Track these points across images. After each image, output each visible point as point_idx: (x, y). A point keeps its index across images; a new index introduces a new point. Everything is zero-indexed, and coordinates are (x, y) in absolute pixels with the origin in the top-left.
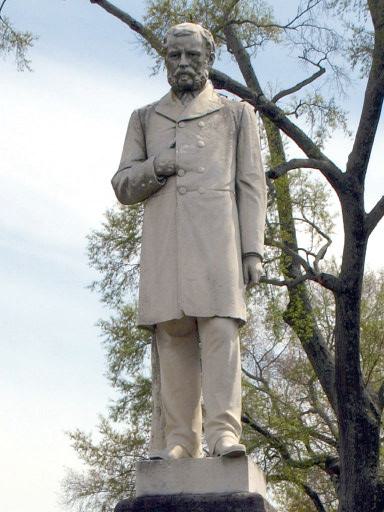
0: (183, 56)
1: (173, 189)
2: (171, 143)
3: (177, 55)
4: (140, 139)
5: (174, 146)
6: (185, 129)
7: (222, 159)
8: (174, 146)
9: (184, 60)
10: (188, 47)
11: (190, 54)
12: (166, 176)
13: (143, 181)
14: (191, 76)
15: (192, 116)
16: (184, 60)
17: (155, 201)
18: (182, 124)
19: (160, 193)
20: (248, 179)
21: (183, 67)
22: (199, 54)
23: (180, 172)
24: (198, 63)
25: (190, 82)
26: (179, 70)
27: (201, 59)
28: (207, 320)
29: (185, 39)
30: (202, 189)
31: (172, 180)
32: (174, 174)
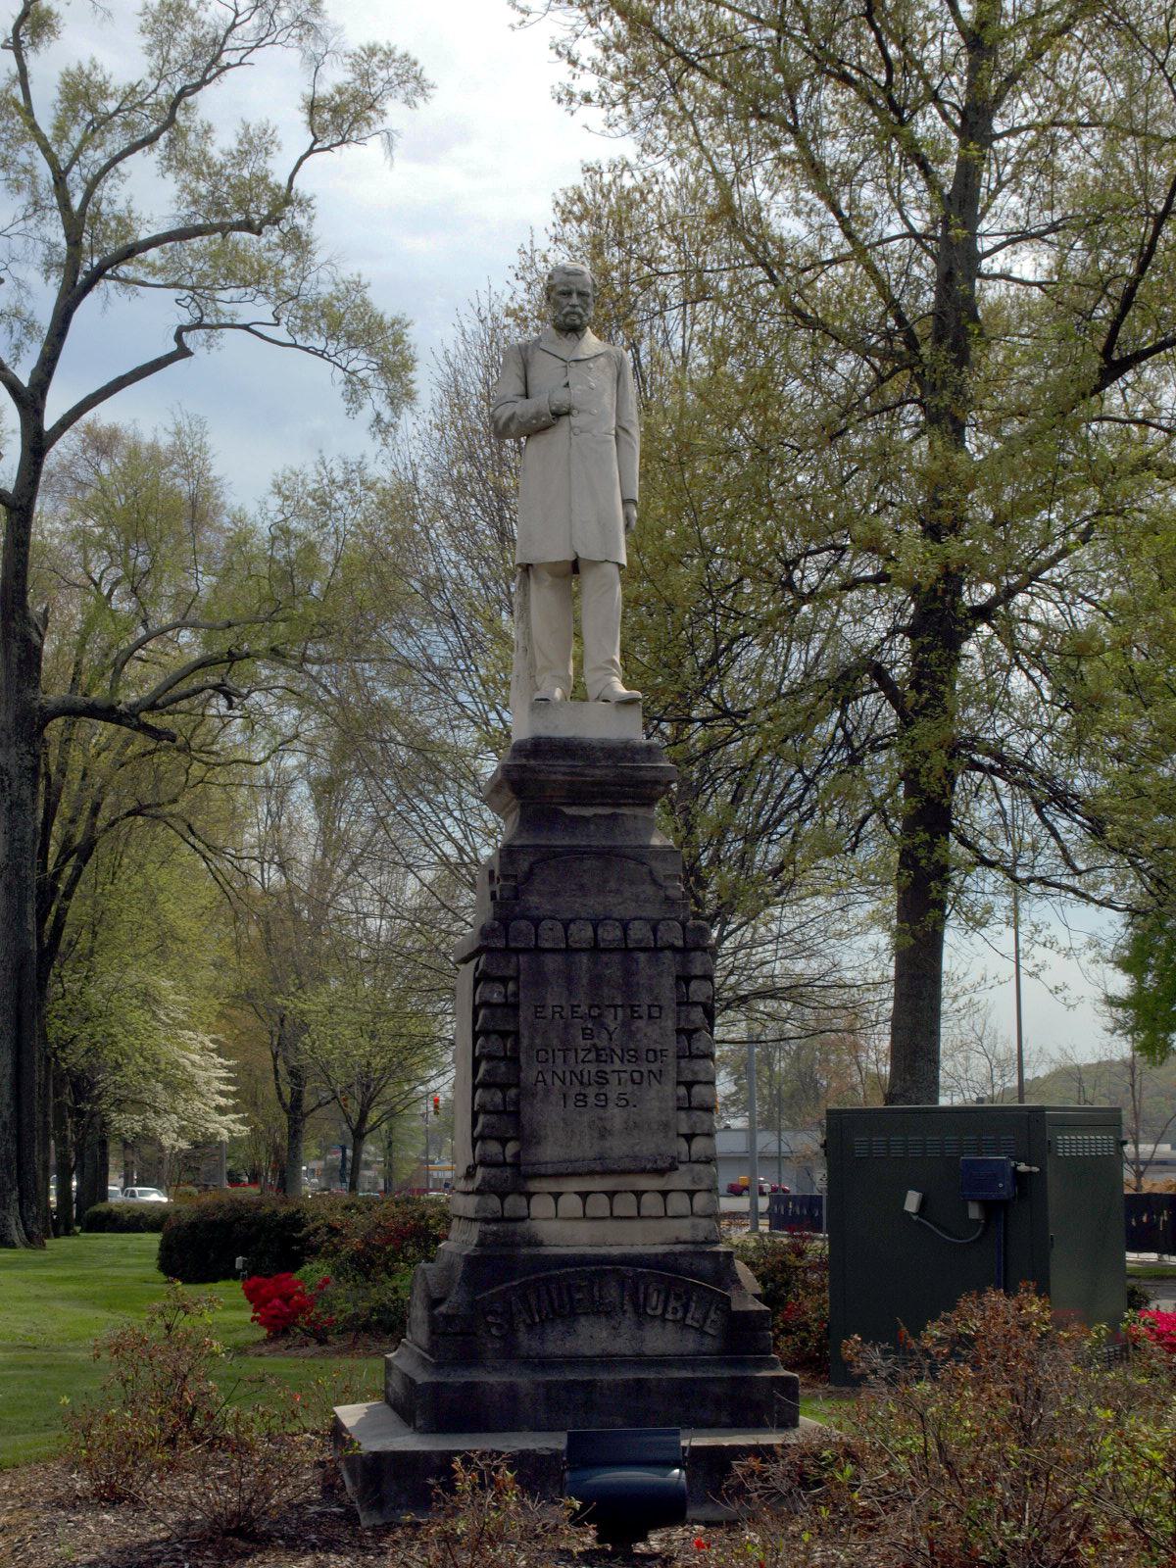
0: (575, 295)
1: (566, 428)
2: (564, 382)
3: (568, 294)
4: (521, 373)
5: (567, 385)
6: (574, 369)
7: (608, 400)
8: (567, 385)
9: (575, 300)
10: (580, 287)
11: (581, 294)
12: (559, 414)
13: (533, 418)
14: (580, 316)
15: (582, 357)
16: (575, 300)
17: (542, 440)
18: (573, 364)
19: (550, 431)
20: (626, 425)
21: (574, 306)
22: (588, 295)
23: (574, 412)
24: (588, 305)
25: (578, 322)
26: (568, 309)
27: (590, 300)
28: (595, 563)
29: (578, 278)
30: (595, 432)
31: (565, 420)
32: (568, 413)
